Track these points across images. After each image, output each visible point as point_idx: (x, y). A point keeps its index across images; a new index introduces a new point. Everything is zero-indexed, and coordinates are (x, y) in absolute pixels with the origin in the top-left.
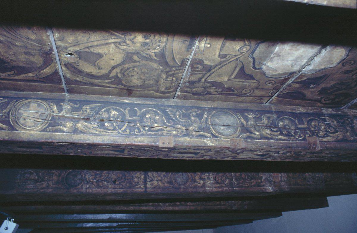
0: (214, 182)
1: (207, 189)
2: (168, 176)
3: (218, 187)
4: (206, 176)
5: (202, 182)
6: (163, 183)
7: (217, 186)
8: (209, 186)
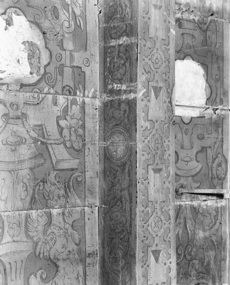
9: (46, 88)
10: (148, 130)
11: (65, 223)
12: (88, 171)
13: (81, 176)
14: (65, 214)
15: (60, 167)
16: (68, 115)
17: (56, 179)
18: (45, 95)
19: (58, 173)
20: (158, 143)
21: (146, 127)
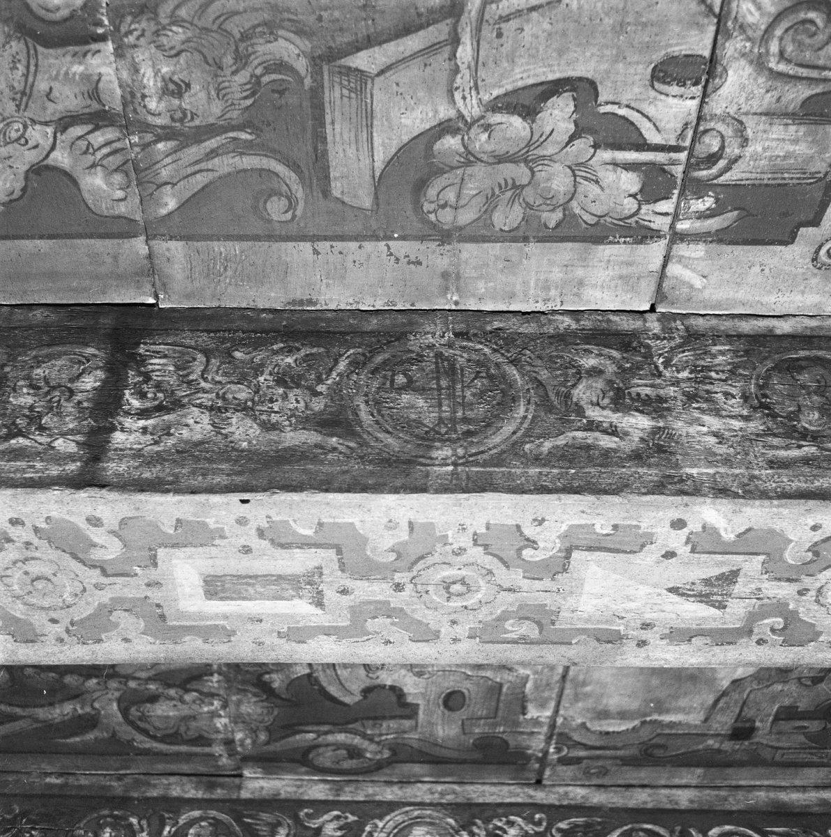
0: (755, 426)
1: (694, 471)
2: (320, 380)
3: (806, 461)
4: (676, 383)
5: (638, 424)
6: (268, 427)
7: (794, 453)
8: (709, 452)
9: (757, 14)
10: (520, 550)
11: (50, 130)
12: (316, 252)
13: (289, 216)
14: (97, 128)
15: (334, 95)
16: (596, 146)
17: (267, 71)
18: (717, 10)
19: (301, 80)
20: (449, 593)
21: (534, 542)
